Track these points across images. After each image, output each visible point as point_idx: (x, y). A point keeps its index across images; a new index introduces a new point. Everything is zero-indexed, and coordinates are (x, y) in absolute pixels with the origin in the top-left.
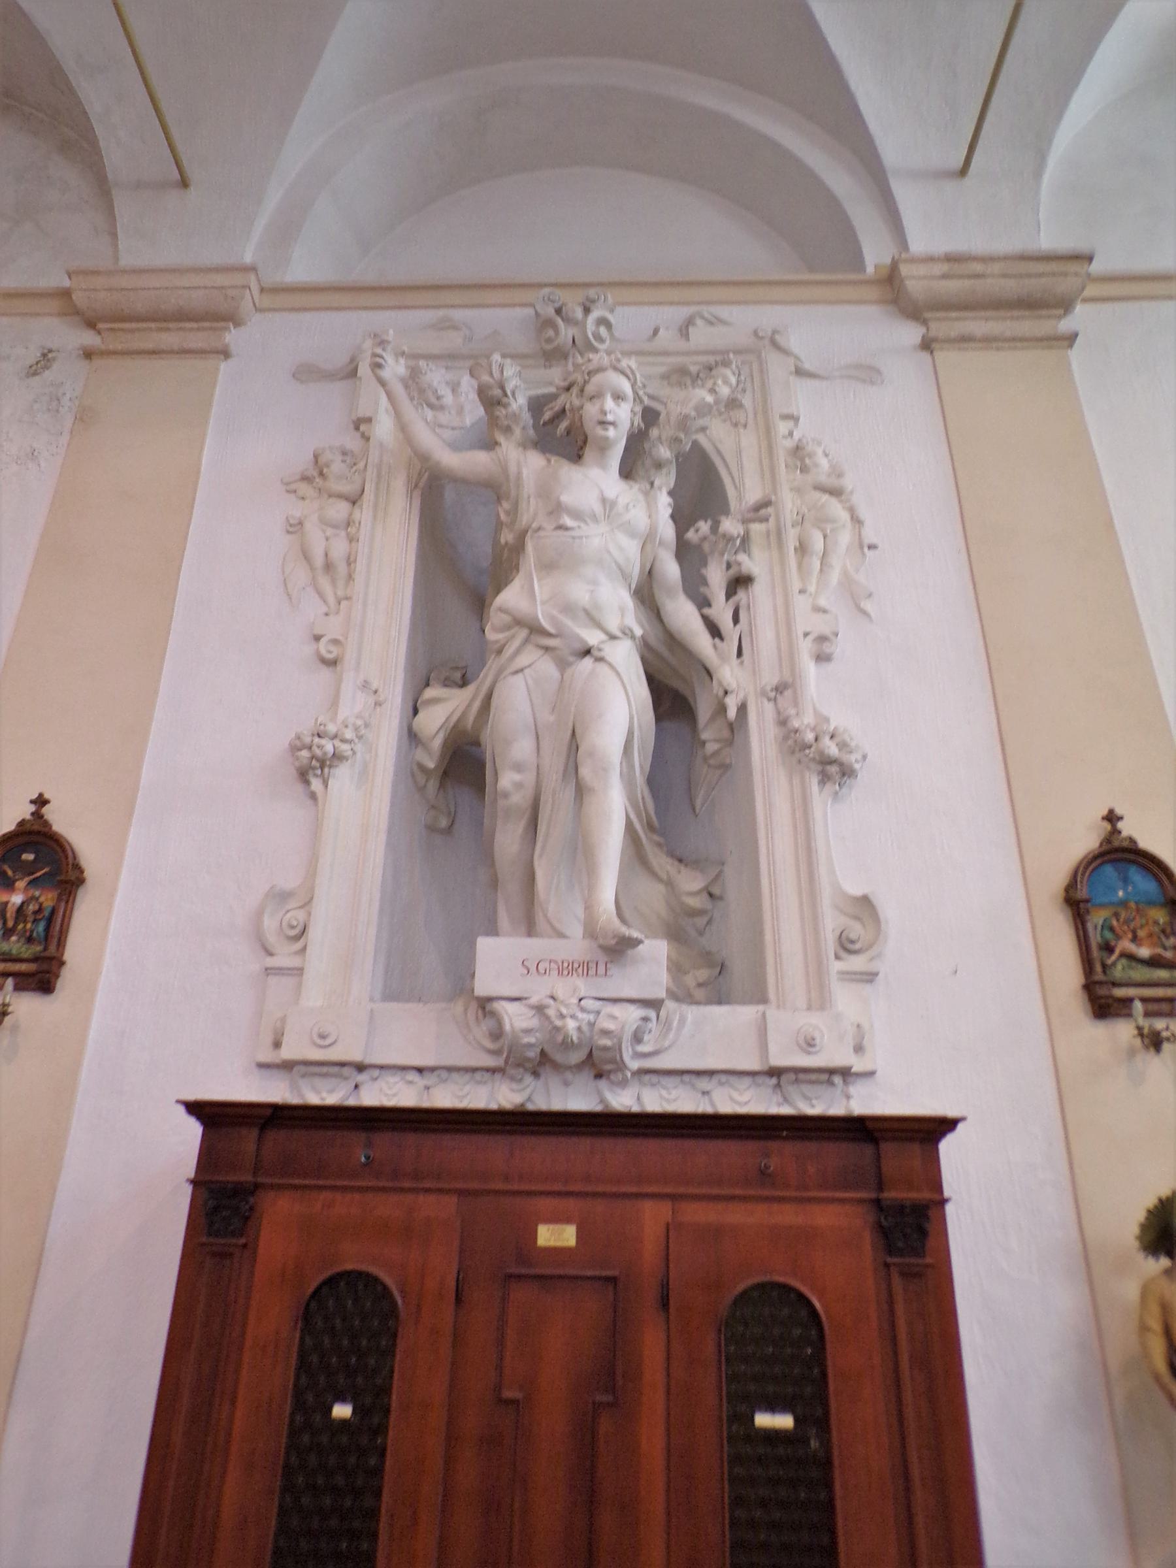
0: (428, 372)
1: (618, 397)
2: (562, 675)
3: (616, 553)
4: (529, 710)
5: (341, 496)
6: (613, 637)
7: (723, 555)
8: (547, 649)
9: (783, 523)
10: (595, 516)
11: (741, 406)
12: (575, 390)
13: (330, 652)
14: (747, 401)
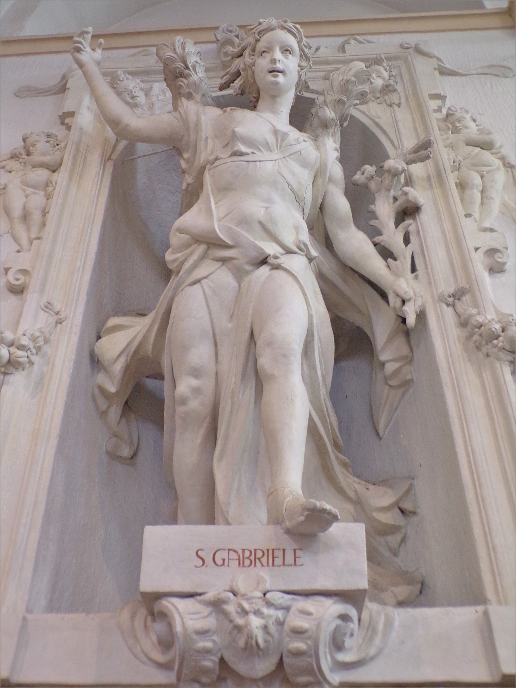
0: (125, 80)
1: (286, 50)
2: (240, 285)
3: (289, 178)
4: (207, 317)
5: (43, 165)
6: (289, 252)
7: (389, 190)
8: (224, 261)
9: (442, 167)
10: (267, 143)
11: (395, 90)
12: (247, 53)
13: (18, 280)
14: (399, 87)
